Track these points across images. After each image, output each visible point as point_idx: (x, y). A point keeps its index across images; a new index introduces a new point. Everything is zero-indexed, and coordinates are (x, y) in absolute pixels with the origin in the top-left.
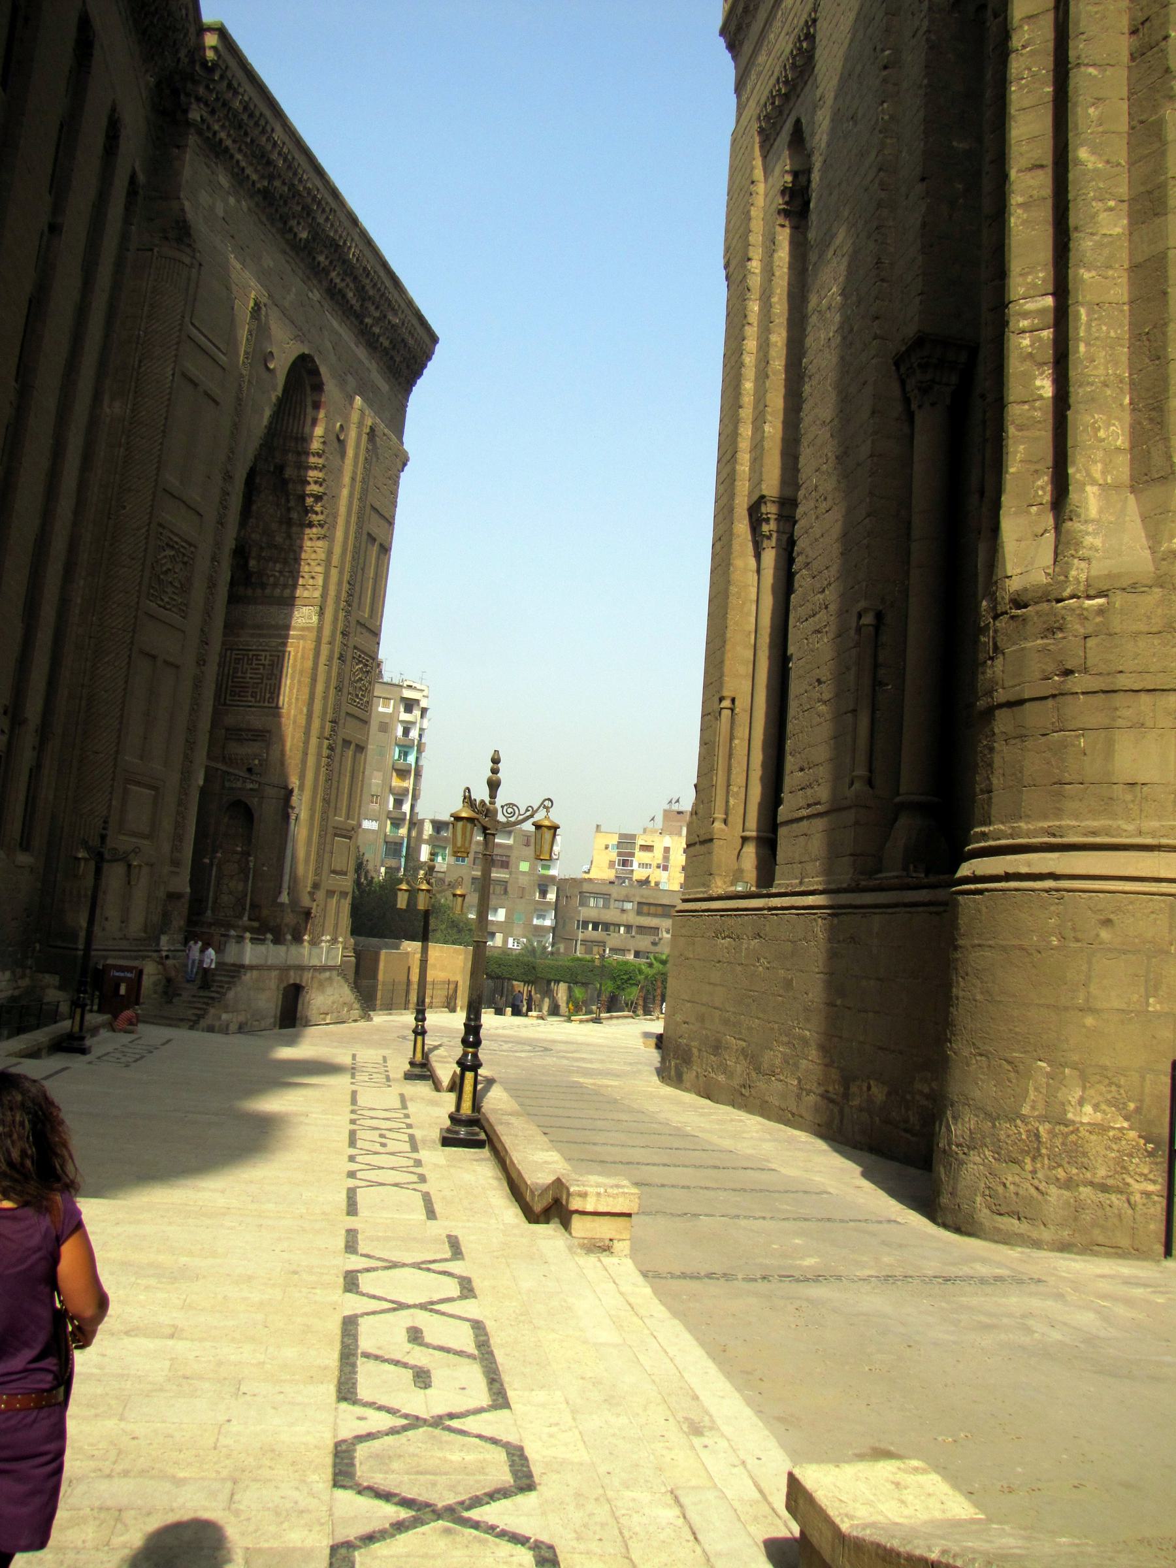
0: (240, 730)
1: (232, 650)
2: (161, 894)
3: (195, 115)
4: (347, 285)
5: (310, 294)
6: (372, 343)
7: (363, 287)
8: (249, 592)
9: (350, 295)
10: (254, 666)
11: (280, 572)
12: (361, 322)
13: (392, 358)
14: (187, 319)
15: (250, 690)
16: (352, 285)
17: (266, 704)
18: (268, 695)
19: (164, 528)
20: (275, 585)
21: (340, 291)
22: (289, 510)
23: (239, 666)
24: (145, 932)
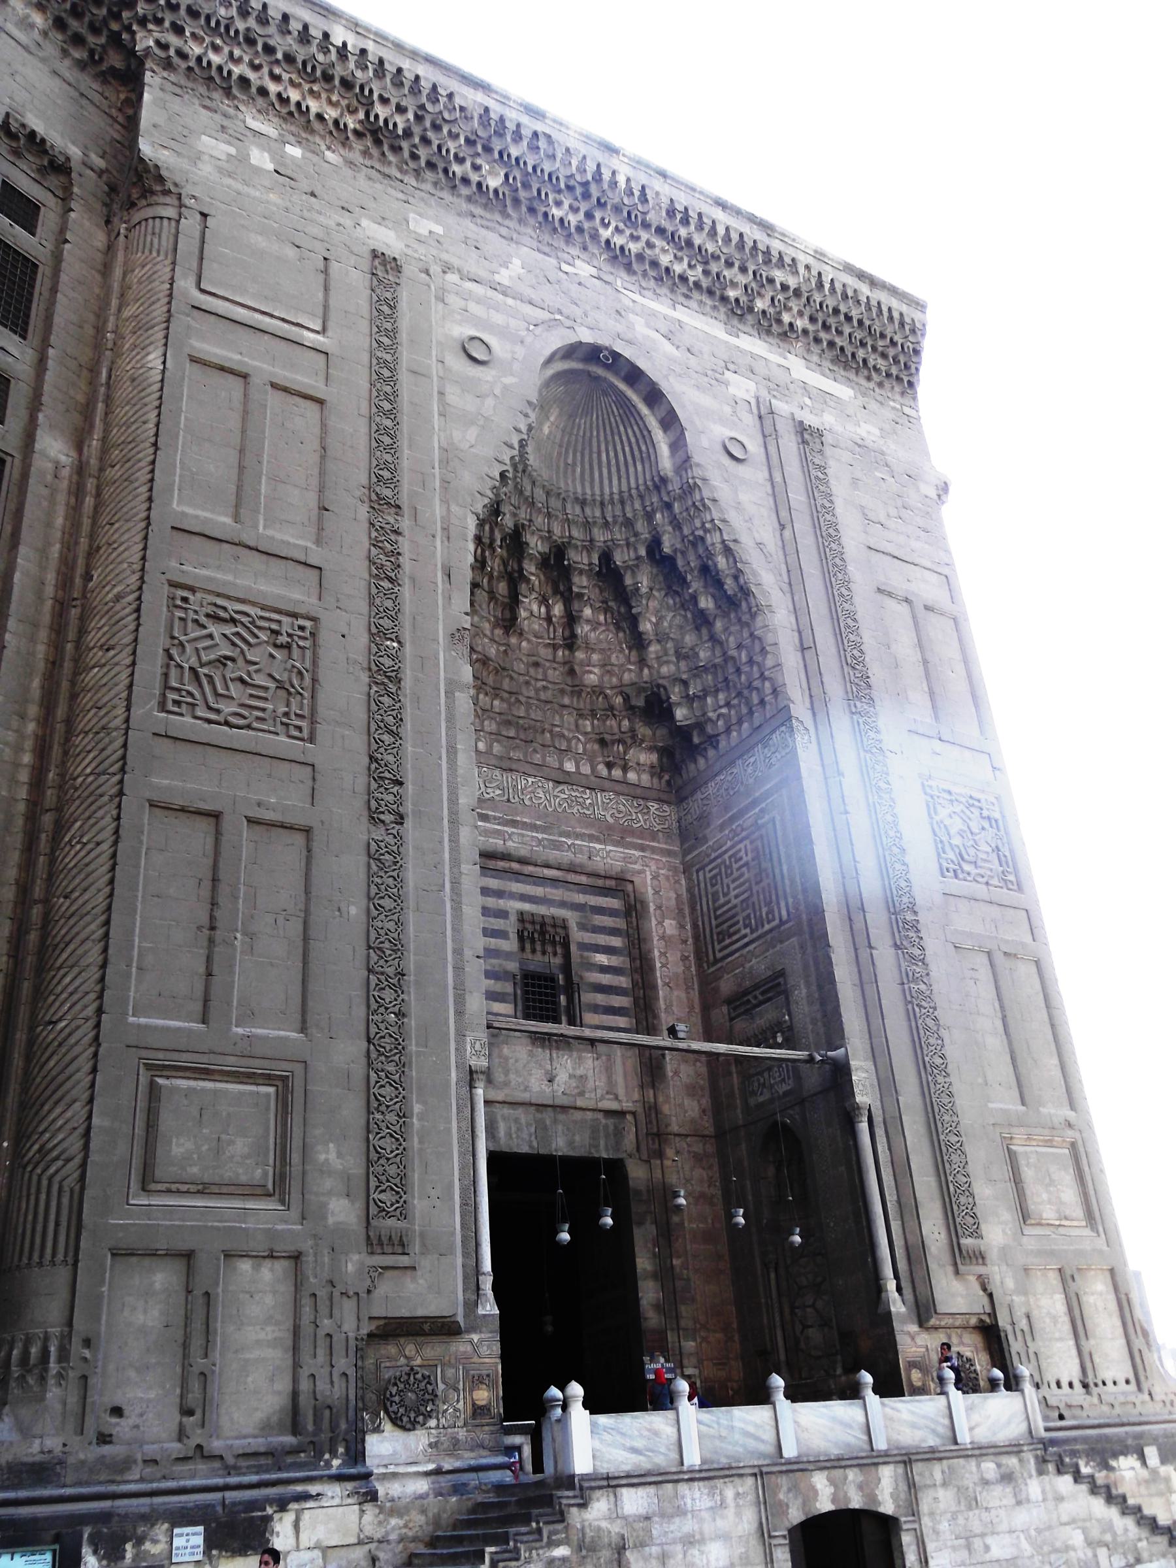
0: (746, 992)
1: (703, 868)
2: (349, 1323)
3: (145, 41)
4: (650, 245)
5: (565, 267)
6: (770, 326)
7: (689, 243)
8: (701, 762)
9: (665, 260)
10: (736, 874)
11: (728, 704)
12: (724, 299)
13: (831, 344)
14: (185, 284)
15: (740, 918)
16: (659, 242)
17: (767, 927)
18: (764, 910)
19: (192, 590)
20: (728, 730)
21: (640, 257)
22: (694, 599)
23: (718, 887)
24: (295, 1429)
